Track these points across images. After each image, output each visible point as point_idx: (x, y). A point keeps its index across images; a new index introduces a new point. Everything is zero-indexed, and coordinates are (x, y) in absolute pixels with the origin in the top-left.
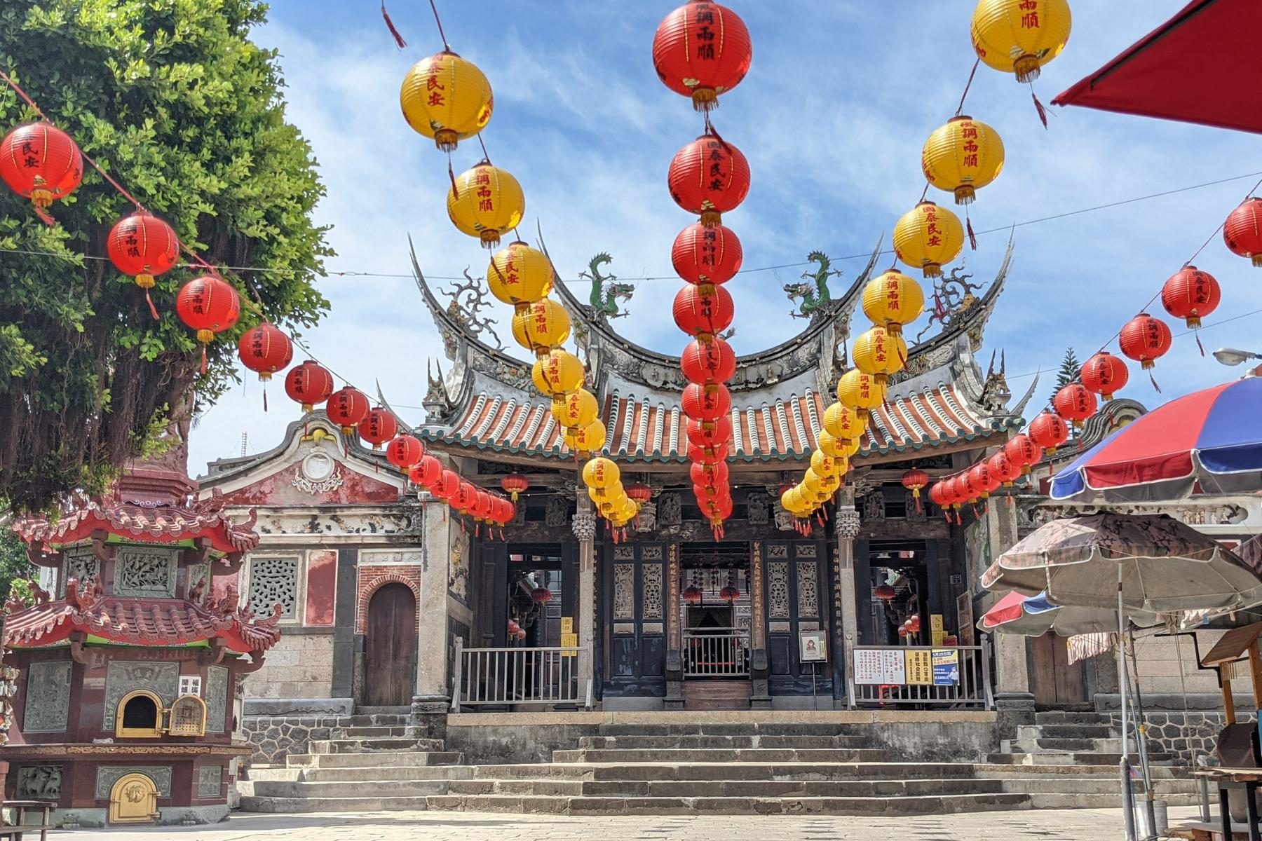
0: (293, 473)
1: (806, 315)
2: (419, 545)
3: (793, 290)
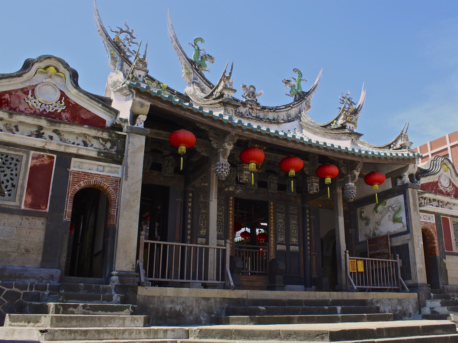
0: (27, 93)
2: (120, 163)
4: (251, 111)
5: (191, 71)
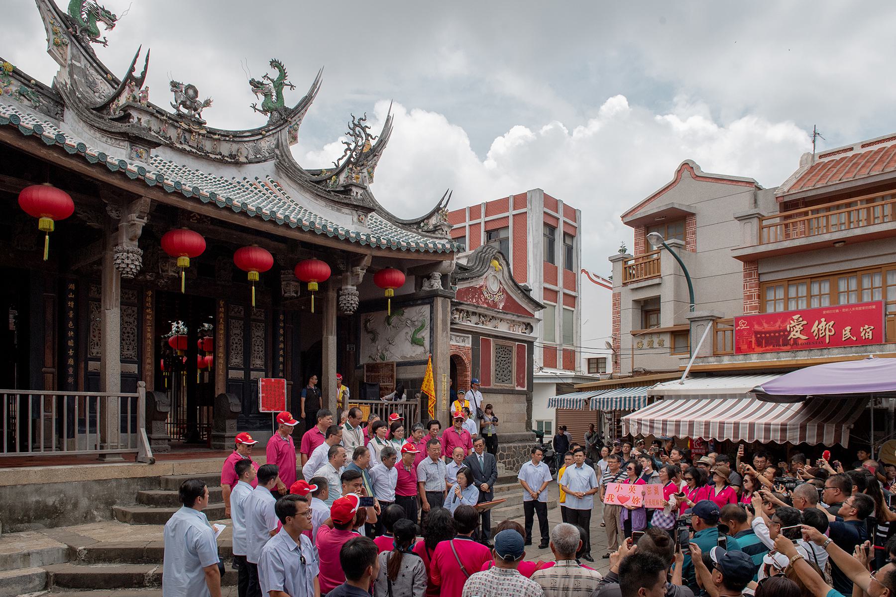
1: (264, 111)
3: (256, 86)
4: (187, 135)
5: (66, 40)
